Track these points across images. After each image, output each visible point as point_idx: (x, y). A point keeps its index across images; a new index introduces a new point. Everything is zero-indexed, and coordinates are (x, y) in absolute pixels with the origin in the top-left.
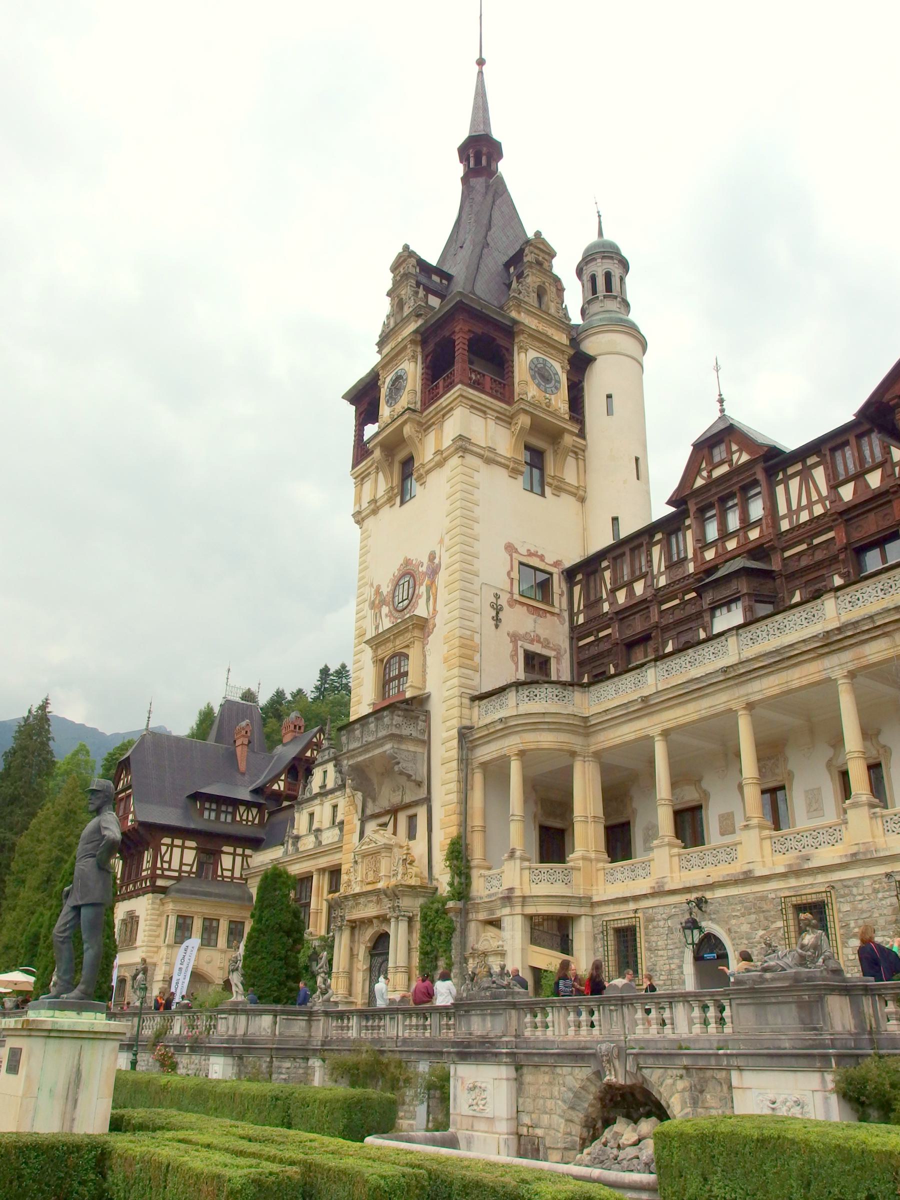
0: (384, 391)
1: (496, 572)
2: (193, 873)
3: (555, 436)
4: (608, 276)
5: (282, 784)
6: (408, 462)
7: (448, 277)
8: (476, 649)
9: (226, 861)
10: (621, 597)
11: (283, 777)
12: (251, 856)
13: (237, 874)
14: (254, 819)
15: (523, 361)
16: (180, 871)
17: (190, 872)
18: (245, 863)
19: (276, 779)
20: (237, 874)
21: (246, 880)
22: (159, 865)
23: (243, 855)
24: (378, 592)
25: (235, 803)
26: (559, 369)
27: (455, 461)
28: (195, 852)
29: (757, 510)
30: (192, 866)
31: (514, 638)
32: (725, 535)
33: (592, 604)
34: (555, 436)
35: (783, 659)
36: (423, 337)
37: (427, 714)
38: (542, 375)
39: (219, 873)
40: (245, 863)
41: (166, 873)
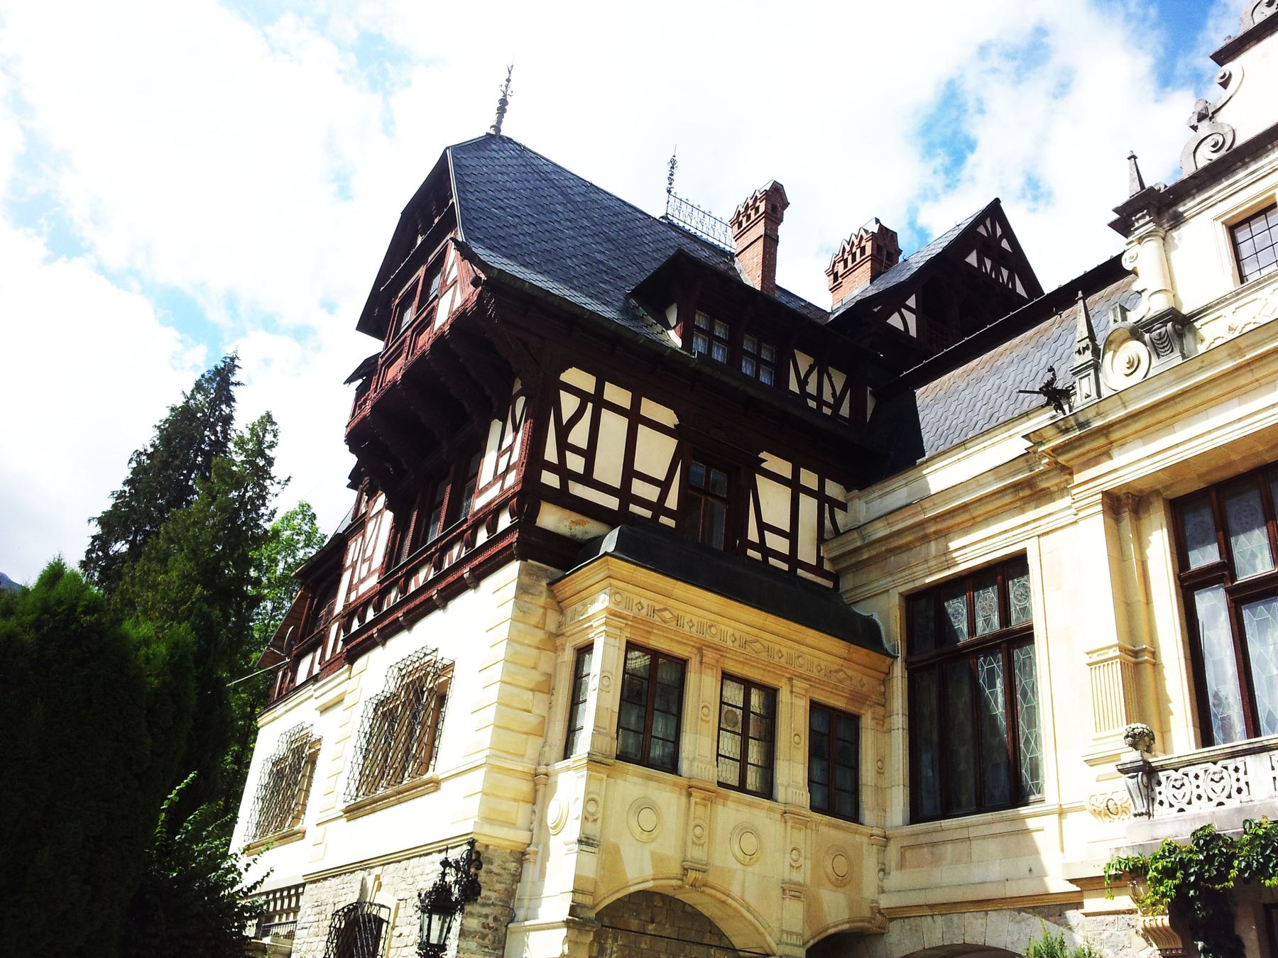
2: (669, 513)
5: (911, 319)
9: (773, 502)
11: (911, 302)
12: (844, 507)
13: (807, 553)
14: (839, 401)
16: (623, 492)
17: (658, 507)
18: (827, 523)
20: (807, 553)
21: (835, 577)
22: (551, 454)
23: (819, 495)
28: (671, 444)
30: (665, 486)
39: (753, 535)
40: (827, 523)
41: (577, 490)
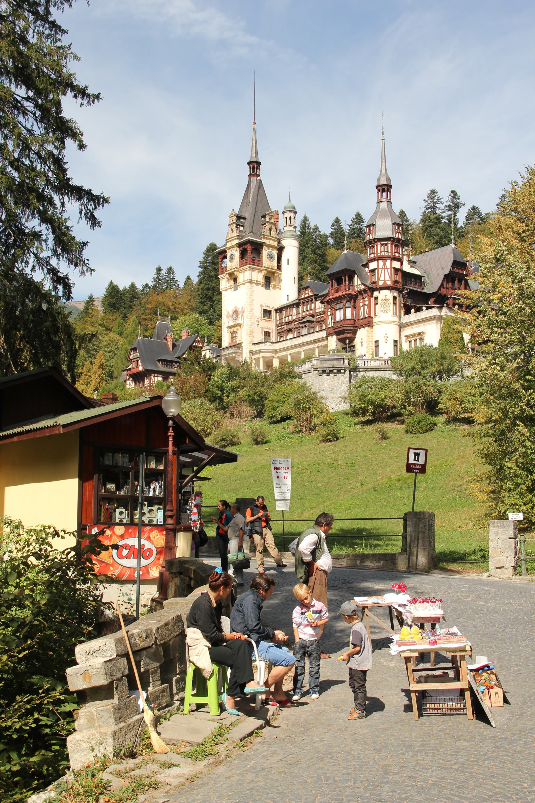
0: (228, 257)
1: (259, 313)
3: (273, 273)
4: (290, 218)
6: (235, 280)
7: (244, 219)
8: (253, 332)
10: (287, 318)
15: (265, 252)
19: (184, 354)
24: (228, 313)
25: (172, 362)
26: (275, 253)
27: (248, 284)
29: (313, 305)
31: (262, 328)
32: (307, 311)
33: (281, 319)
34: (273, 273)
35: (308, 343)
36: (239, 245)
37: (242, 347)
38: (270, 257)
